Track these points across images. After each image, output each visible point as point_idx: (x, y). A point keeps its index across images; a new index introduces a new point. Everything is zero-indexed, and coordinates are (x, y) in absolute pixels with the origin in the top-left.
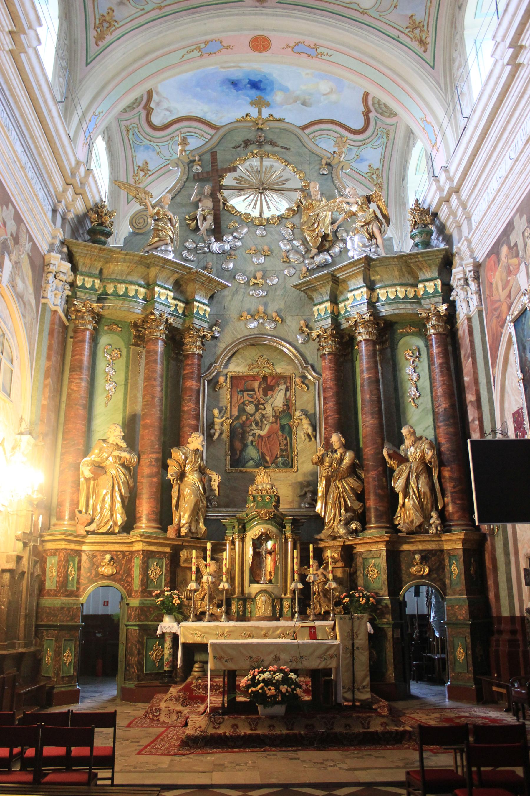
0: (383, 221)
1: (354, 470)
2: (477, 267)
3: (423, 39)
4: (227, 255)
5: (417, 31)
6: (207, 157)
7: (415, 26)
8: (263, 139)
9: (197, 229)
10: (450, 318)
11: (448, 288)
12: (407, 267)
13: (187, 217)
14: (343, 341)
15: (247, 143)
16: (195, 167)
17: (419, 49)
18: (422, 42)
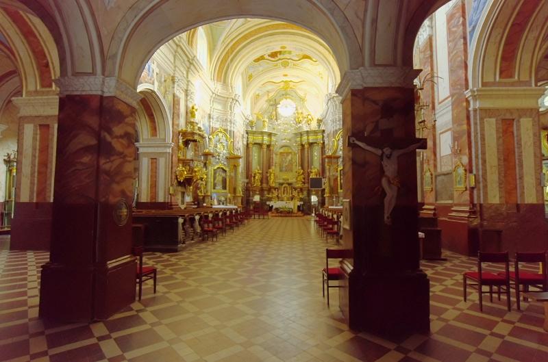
1: (303, 174)
2: (328, 134)
4: (279, 125)
10: (324, 143)
11: (323, 137)
12: (315, 132)
14: (303, 146)
15: (283, 95)
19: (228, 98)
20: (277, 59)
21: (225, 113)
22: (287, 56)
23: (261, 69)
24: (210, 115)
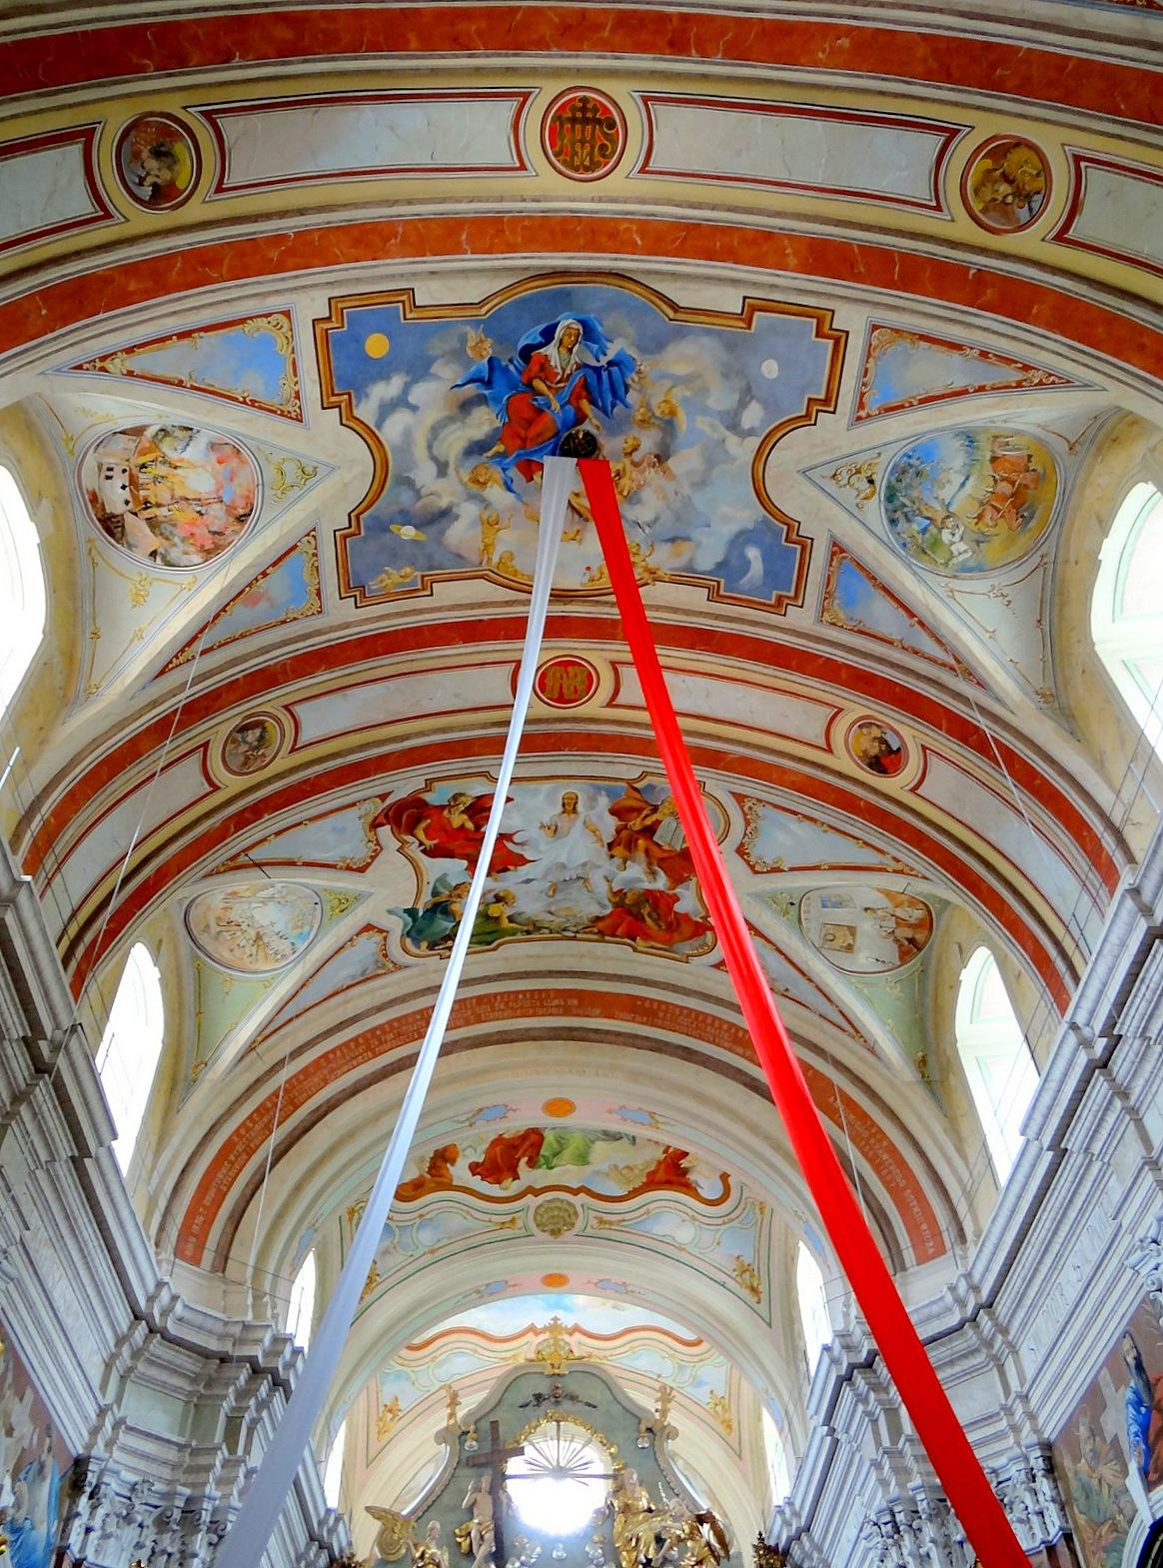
0: (722, 1553)
3: (755, 1285)
5: (747, 1276)
6: (485, 1425)
7: (744, 1269)
8: (560, 1392)
9: (470, 1554)
13: (457, 1531)
15: (539, 1398)
16: (468, 1444)
17: (752, 1300)
18: (754, 1290)
19: (224, 1359)
20: (512, 1187)
21: (193, 1458)
22: (566, 1173)
23: (426, 1237)
24: (80, 1465)
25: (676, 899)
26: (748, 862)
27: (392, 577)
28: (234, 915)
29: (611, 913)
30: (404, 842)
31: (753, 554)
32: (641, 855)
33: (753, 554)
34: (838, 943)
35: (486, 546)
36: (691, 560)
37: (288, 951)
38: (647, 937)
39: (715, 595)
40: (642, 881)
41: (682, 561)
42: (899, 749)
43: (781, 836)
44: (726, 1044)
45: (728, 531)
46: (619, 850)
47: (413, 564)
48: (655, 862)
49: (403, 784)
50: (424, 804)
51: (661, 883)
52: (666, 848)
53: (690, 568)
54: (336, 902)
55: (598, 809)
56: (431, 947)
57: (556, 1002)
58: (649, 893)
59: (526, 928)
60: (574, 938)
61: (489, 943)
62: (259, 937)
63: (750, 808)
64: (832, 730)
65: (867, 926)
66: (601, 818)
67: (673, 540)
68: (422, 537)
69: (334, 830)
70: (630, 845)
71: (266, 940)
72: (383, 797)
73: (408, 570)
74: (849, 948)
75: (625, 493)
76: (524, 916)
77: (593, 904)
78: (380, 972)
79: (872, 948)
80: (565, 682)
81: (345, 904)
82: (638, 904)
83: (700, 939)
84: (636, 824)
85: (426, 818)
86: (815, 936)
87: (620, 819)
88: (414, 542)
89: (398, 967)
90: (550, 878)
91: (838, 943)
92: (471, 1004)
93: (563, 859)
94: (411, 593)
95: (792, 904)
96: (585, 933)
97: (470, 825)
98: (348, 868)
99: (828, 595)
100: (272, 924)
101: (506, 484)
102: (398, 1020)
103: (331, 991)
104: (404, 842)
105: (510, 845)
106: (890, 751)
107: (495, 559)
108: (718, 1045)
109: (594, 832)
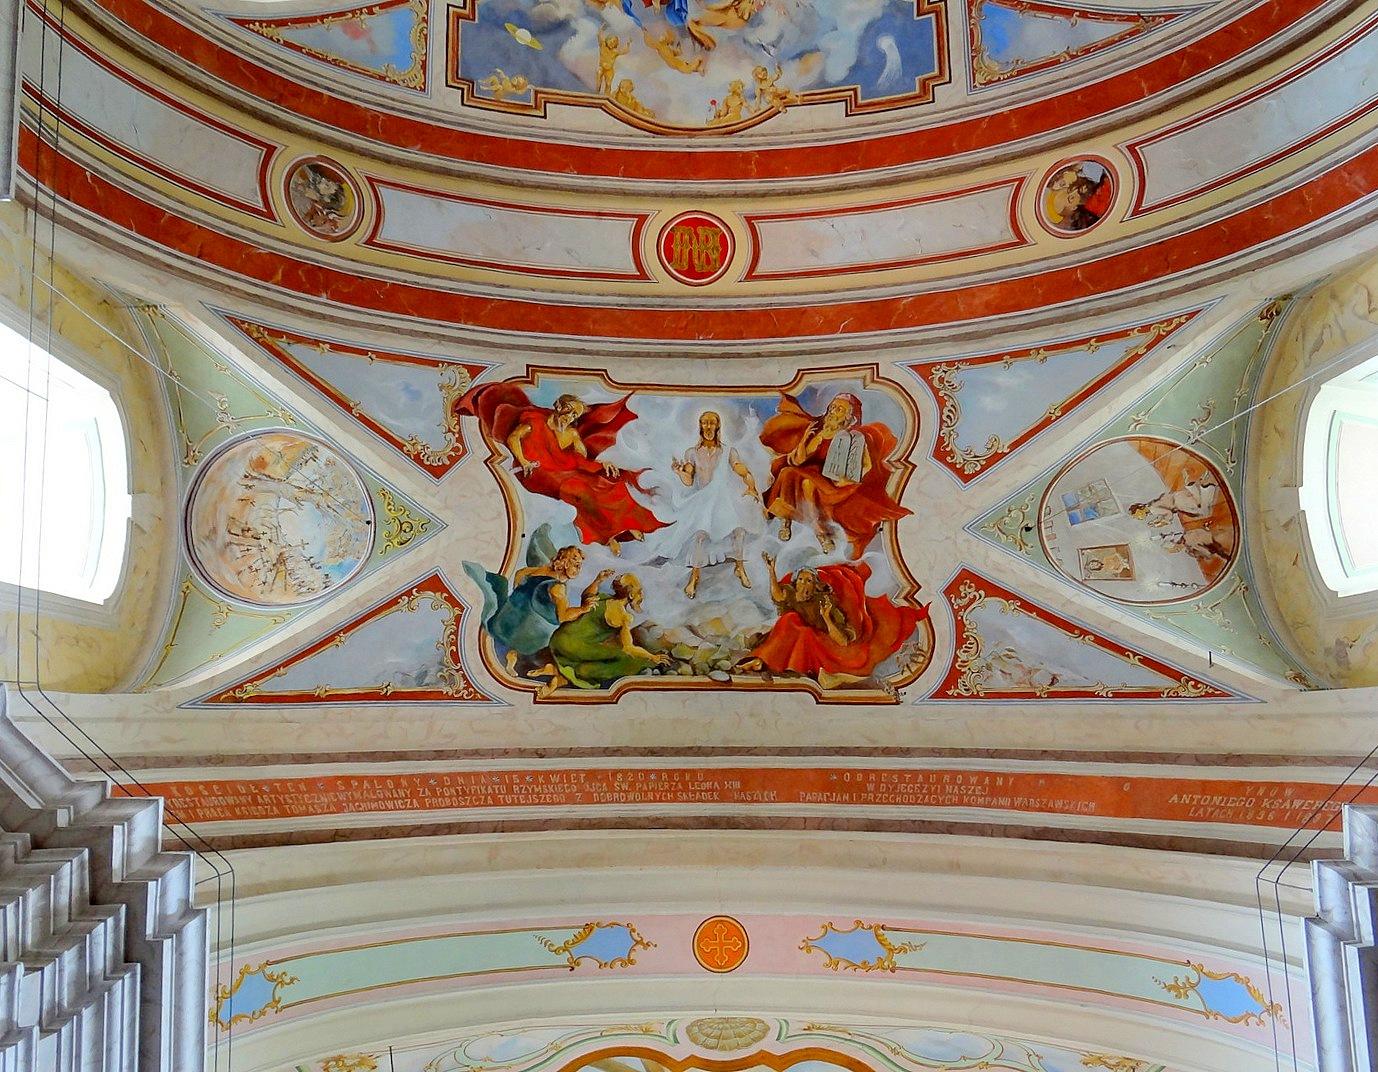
25: (865, 572)
26: (952, 466)
27: (502, 83)
28: (254, 518)
29: (778, 626)
30: (494, 452)
31: (887, 43)
32: (809, 505)
33: (887, 43)
34: (1109, 570)
35: (605, 71)
36: (823, 73)
37: (318, 584)
38: (835, 666)
39: (853, 107)
40: (815, 553)
41: (811, 78)
42: (1104, 176)
43: (989, 402)
44: (981, 800)
45: (855, 28)
46: (779, 504)
47: (526, 74)
48: (829, 513)
49: (503, 360)
50: (523, 400)
51: (841, 551)
52: (841, 483)
53: (822, 82)
54: (396, 526)
55: (745, 440)
56: (523, 668)
57: (708, 785)
58: (828, 572)
59: (658, 659)
60: (727, 686)
61: (606, 685)
62: (281, 560)
63: (941, 380)
64: (1018, 215)
65: (1142, 539)
66: (750, 451)
67: (800, 55)
68: (537, 46)
69: (407, 388)
70: (793, 493)
71: (290, 565)
72: (474, 371)
73: (521, 80)
74: (1127, 574)
75: (746, 17)
76: (657, 632)
77: (749, 614)
78: (446, 689)
79: (1161, 566)
80: (695, 247)
81: (409, 528)
82: (811, 600)
83: (910, 642)
84: (798, 454)
85: (526, 422)
86: (1071, 566)
87: (777, 451)
88: (528, 48)
89: (477, 696)
90: (689, 559)
91: (1109, 570)
92: (577, 778)
93: (705, 525)
94: (522, 109)
95: (1028, 529)
96: (744, 672)
97: (581, 448)
98: (418, 459)
99: (974, 52)
100: (304, 544)
101: (624, 6)
102: (466, 775)
103: (364, 684)
104: (494, 452)
105: (633, 492)
106: (1093, 187)
107: (614, 88)
108: (969, 805)
109: (744, 476)
